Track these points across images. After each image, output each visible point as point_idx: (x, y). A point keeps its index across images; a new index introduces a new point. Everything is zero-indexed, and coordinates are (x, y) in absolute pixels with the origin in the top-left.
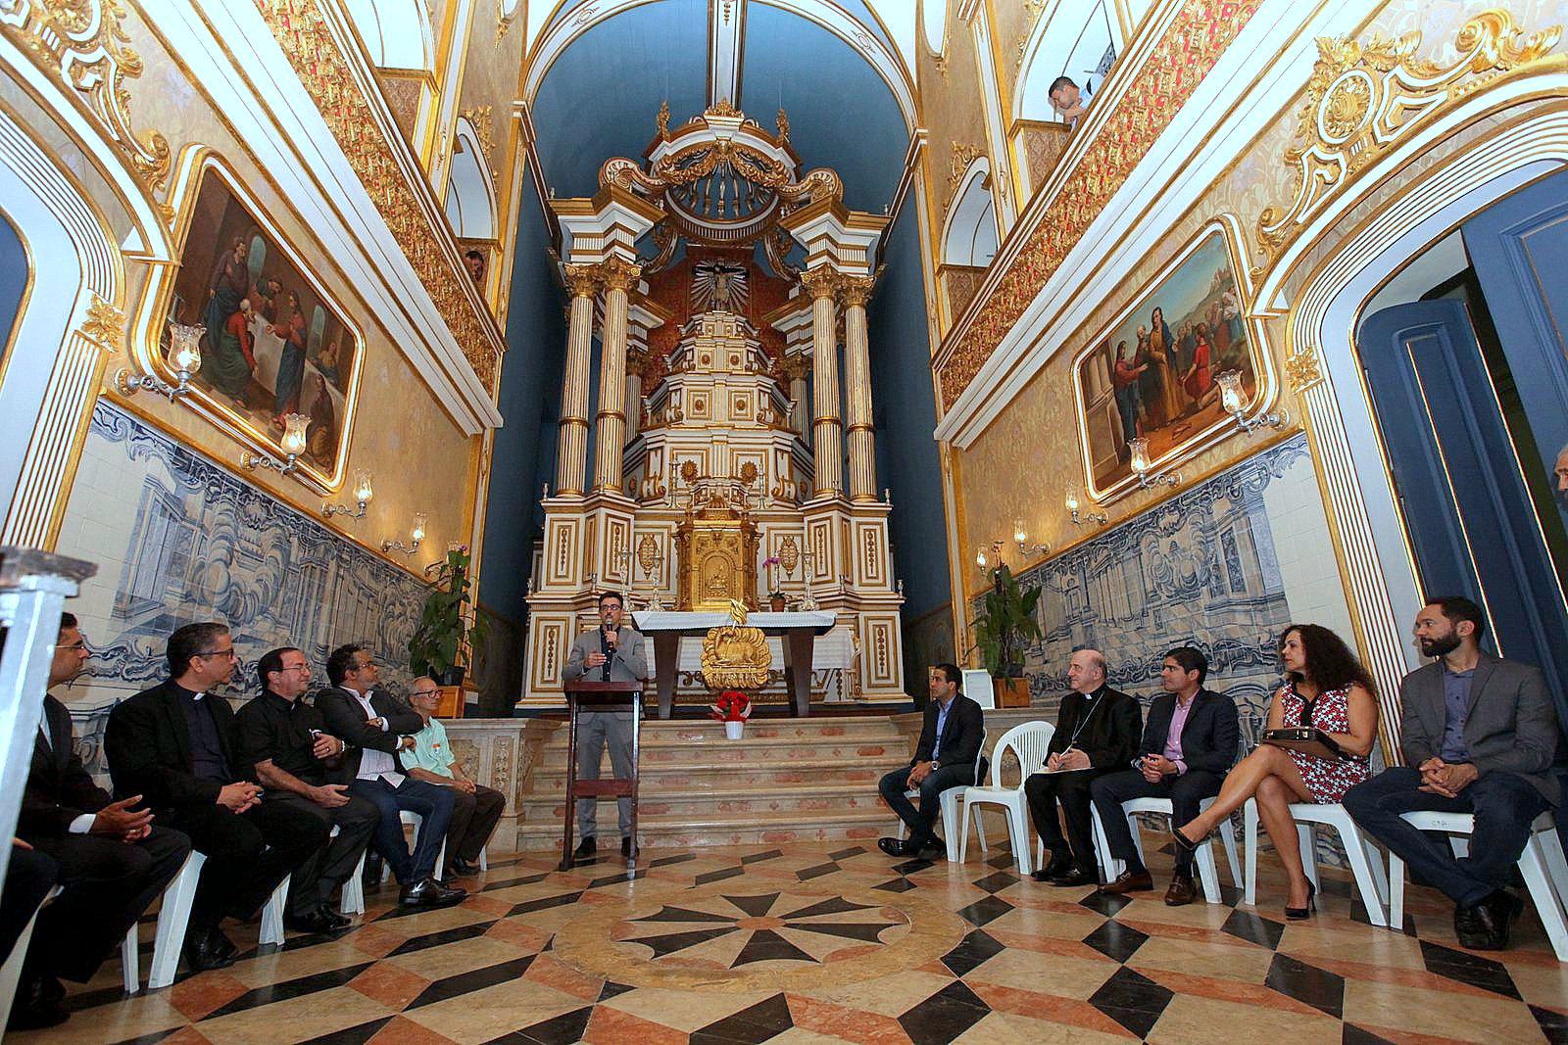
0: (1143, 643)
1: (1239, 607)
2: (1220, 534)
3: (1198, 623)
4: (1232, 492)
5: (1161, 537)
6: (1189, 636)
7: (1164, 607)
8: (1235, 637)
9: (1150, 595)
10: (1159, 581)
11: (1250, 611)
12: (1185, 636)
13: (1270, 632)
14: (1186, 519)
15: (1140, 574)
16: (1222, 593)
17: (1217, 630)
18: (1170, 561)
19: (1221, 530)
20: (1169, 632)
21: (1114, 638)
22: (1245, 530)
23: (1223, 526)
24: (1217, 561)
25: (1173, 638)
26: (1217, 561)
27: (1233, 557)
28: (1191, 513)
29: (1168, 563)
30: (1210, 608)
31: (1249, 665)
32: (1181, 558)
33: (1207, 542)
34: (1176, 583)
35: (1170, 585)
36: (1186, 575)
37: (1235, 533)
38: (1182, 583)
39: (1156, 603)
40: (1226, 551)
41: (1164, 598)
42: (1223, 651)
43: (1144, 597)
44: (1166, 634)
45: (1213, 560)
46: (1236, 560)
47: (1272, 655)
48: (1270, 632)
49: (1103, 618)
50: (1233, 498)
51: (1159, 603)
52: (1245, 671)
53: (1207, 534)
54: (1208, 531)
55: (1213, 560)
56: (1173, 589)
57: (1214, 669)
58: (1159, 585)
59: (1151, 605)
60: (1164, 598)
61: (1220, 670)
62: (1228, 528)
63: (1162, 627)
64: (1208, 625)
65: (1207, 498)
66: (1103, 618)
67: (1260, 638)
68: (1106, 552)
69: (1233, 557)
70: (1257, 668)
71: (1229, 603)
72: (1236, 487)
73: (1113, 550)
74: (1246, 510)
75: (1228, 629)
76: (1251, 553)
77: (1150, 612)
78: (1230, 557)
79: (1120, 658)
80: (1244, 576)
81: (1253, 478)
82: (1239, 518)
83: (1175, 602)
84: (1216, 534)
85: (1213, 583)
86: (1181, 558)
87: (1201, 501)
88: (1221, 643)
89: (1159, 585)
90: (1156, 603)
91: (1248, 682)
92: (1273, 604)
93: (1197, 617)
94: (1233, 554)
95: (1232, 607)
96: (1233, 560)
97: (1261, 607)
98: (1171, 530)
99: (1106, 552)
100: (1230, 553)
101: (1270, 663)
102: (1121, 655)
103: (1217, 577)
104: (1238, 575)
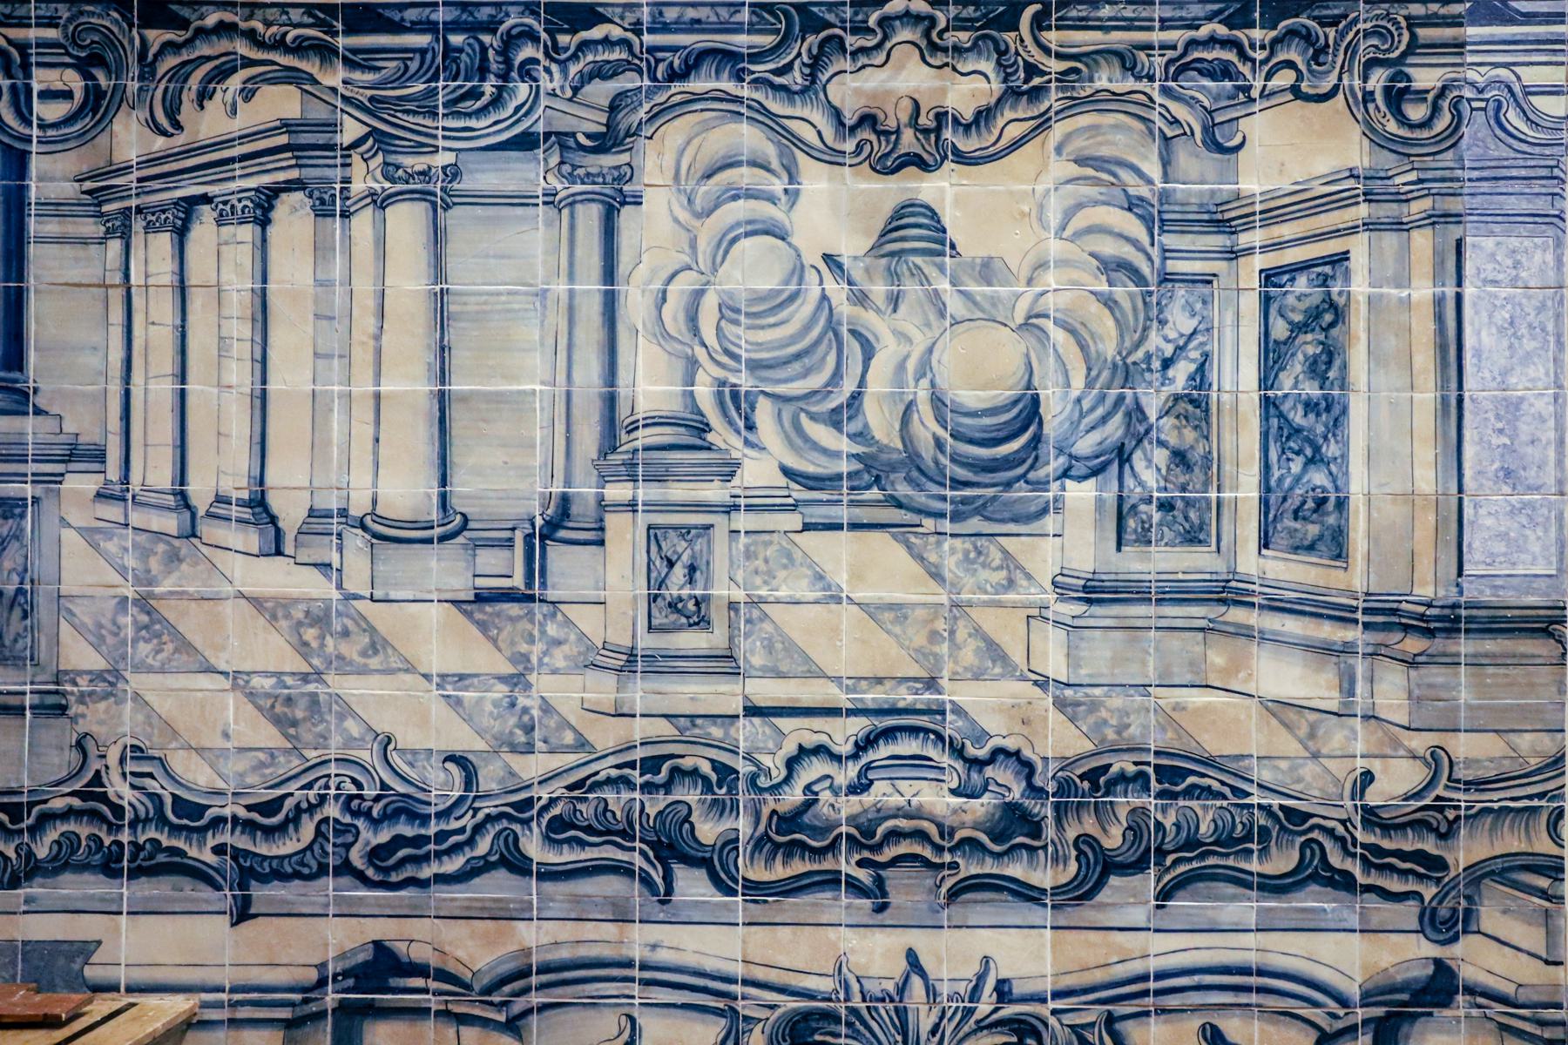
0: (517, 681)
1: (1292, 626)
2: (1259, 262)
3: (994, 650)
4: (1396, 97)
5: (832, 158)
6: (905, 697)
7: (742, 521)
8: (1214, 745)
9: (644, 437)
10: (744, 381)
11: (1347, 649)
12: (872, 697)
13: (1436, 760)
14: (1043, 124)
15: (591, 310)
16: (1193, 537)
17: (1117, 701)
18: (861, 299)
19: (1266, 248)
20: (753, 654)
21: (231, 611)
22: (1422, 291)
23: (1287, 231)
24: (1200, 376)
25: (767, 691)
26: (1200, 376)
27: (1312, 390)
28: (1075, 105)
29: (844, 309)
30: (1094, 592)
31: (1273, 886)
32: (955, 305)
33: (1166, 278)
34: (880, 420)
35: (834, 419)
36: (970, 398)
37: (1360, 287)
38: (926, 428)
39: (678, 492)
40: (1273, 356)
41: (759, 472)
42: (1124, 802)
43: (588, 438)
44: (726, 663)
45: (1181, 373)
46: (1332, 411)
47: (1419, 856)
48: (1436, 760)
49: (155, 471)
50: (1392, 126)
51: (714, 492)
52: (1244, 908)
53: (1170, 241)
54: (1184, 225)
55: (1181, 373)
56: (845, 445)
57: (1044, 877)
58: (736, 403)
59: (645, 492)
60: (759, 472)
61: (1082, 891)
62: (1332, 247)
63: (701, 621)
64: (1055, 666)
65: (1224, 71)
66: (155, 471)
67: (1368, 777)
68: (281, 103)
69: (1312, 390)
70: (1312, 900)
71: (1227, 593)
72: (1426, 77)
73: (374, 107)
74: (1454, 205)
75: (1177, 707)
76: (1427, 397)
77: (625, 534)
78: (1294, 383)
79: (269, 736)
80: (1357, 487)
81: (1531, 76)
82: (1398, 226)
83: (844, 514)
84: (1233, 254)
85: (1149, 470)
86: (955, 305)
87: (1180, 68)
88: (1123, 764)
89: (736, 403)
90: (678, 492)
91: (1252, 959)
92: (1490, 645)
93: (990, 621)
94: (1318, 368)
95: (1237, 615)
96: (1310, 406)
97: (1413, 644)
98: (909, 142)
99: (281, 103)
100: (1297, 366)
101: (1395, 885)
102: (278, 721)
103: (1180, 457)
104: (1318, 478)
